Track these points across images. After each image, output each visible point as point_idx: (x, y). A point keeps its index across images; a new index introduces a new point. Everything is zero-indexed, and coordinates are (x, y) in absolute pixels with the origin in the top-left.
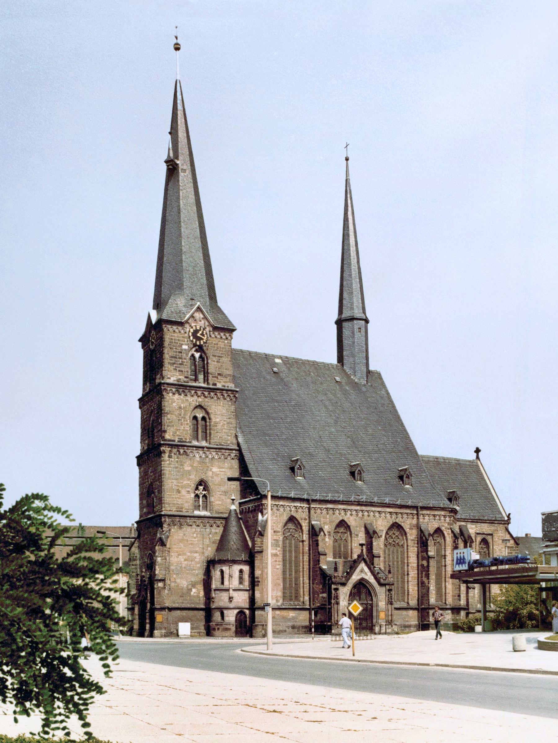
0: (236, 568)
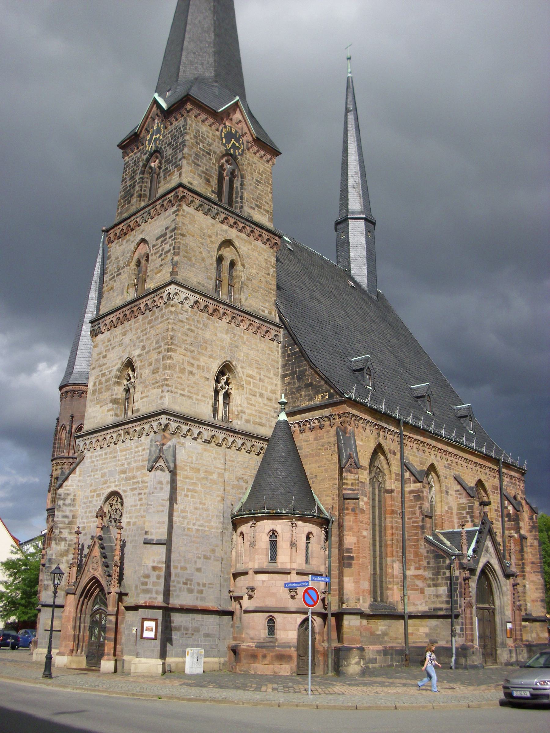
0: (305, 527)
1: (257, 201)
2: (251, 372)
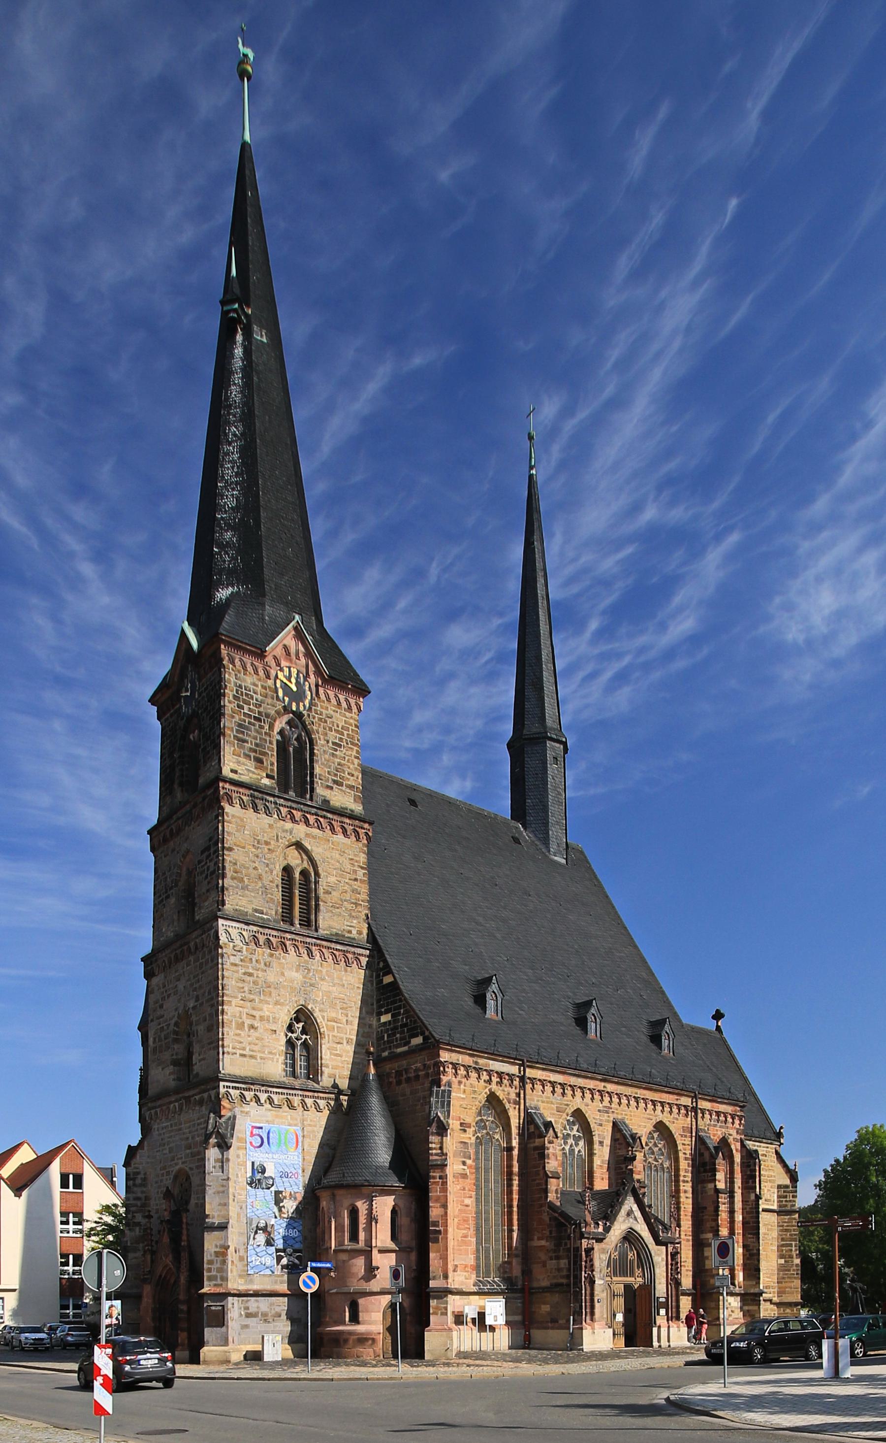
2: (334, 1015)
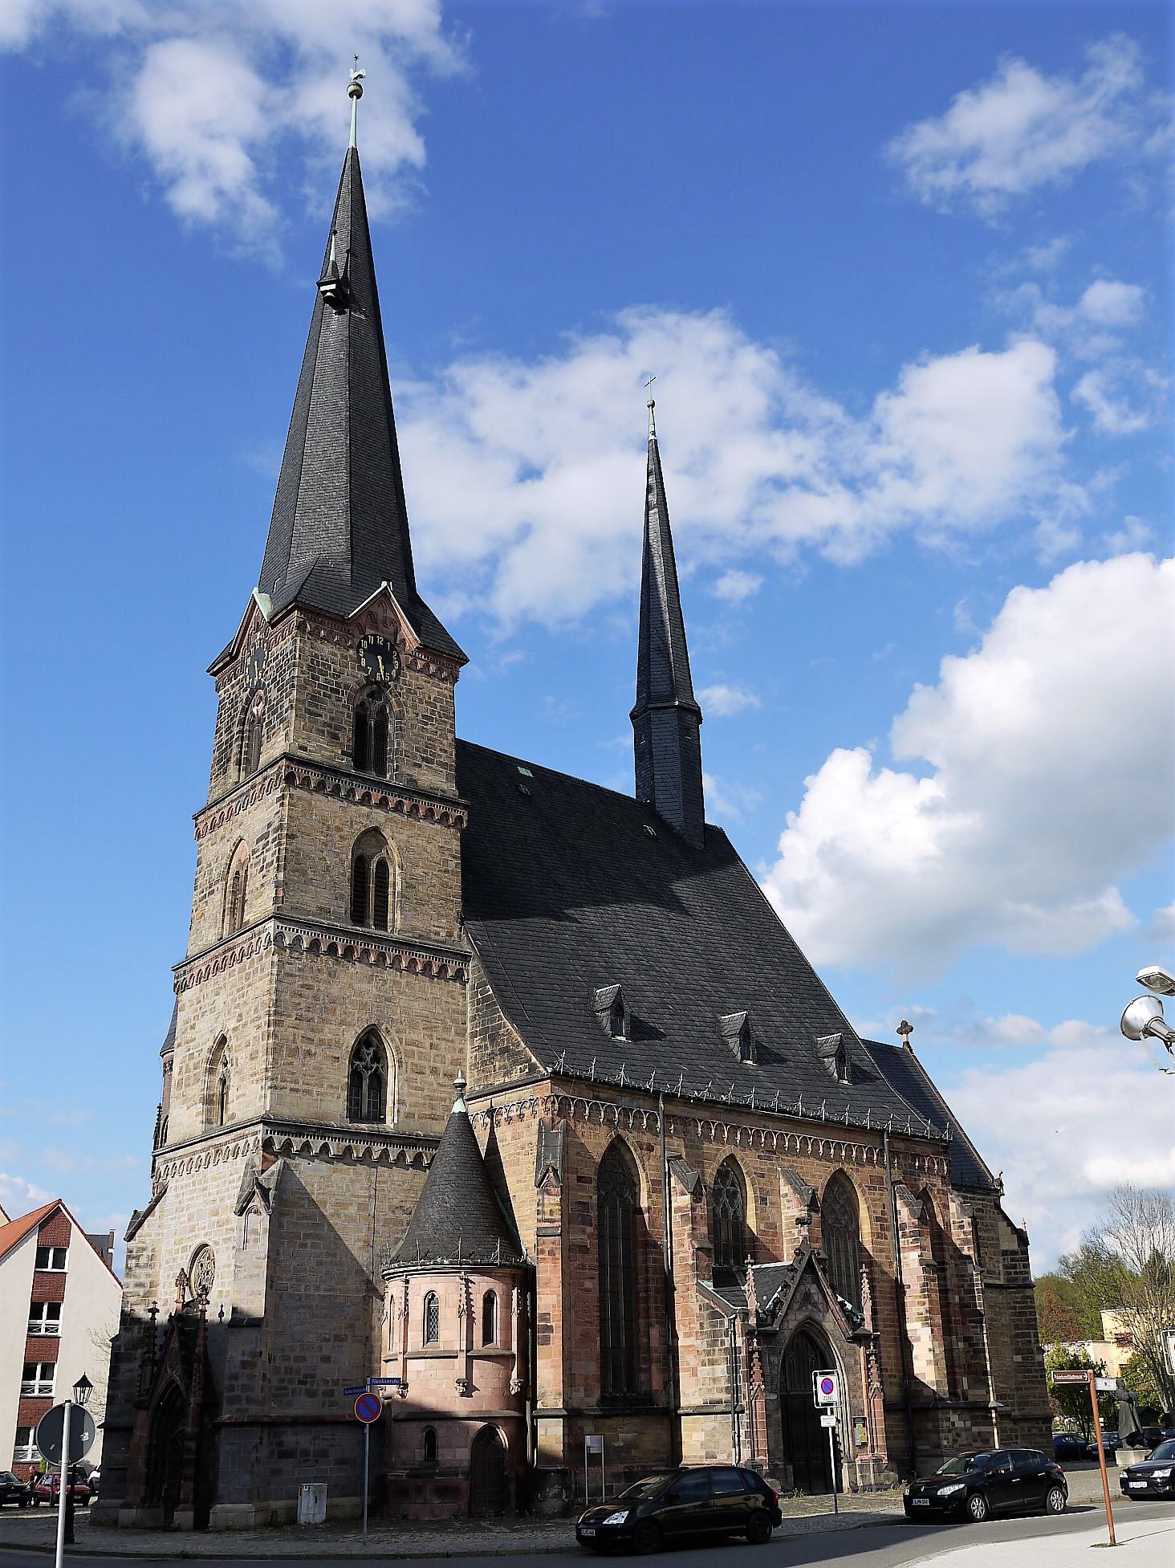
0: (482, 1285)
1: (425, 752)
2: (414, 1037)
